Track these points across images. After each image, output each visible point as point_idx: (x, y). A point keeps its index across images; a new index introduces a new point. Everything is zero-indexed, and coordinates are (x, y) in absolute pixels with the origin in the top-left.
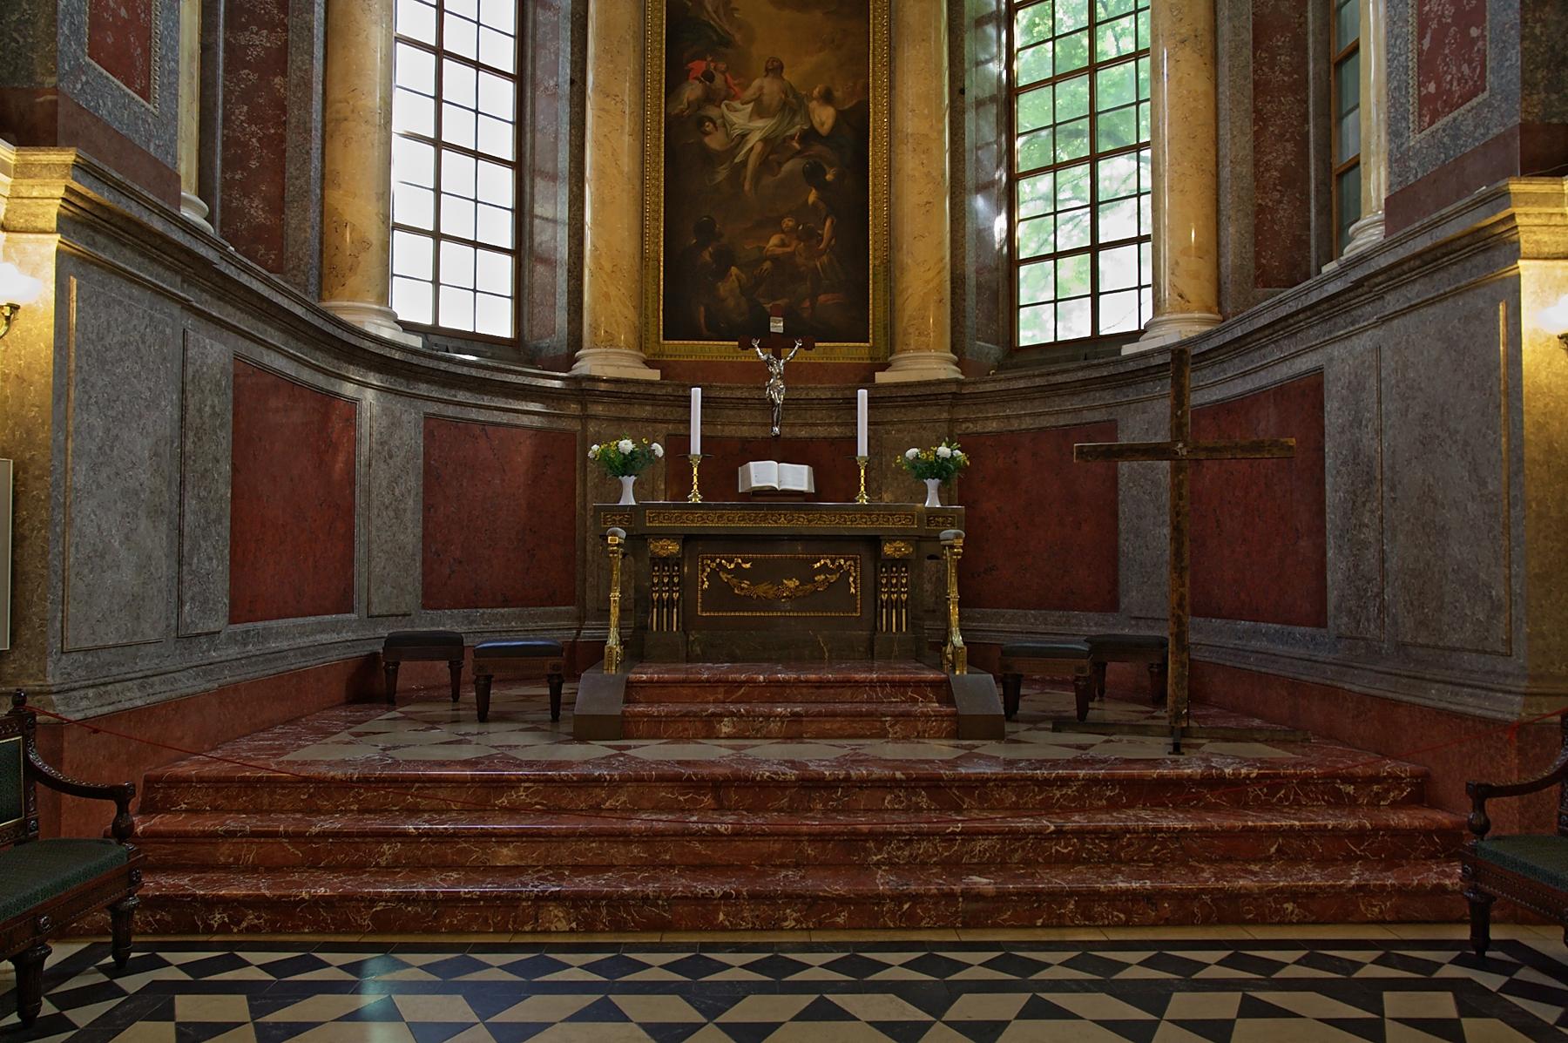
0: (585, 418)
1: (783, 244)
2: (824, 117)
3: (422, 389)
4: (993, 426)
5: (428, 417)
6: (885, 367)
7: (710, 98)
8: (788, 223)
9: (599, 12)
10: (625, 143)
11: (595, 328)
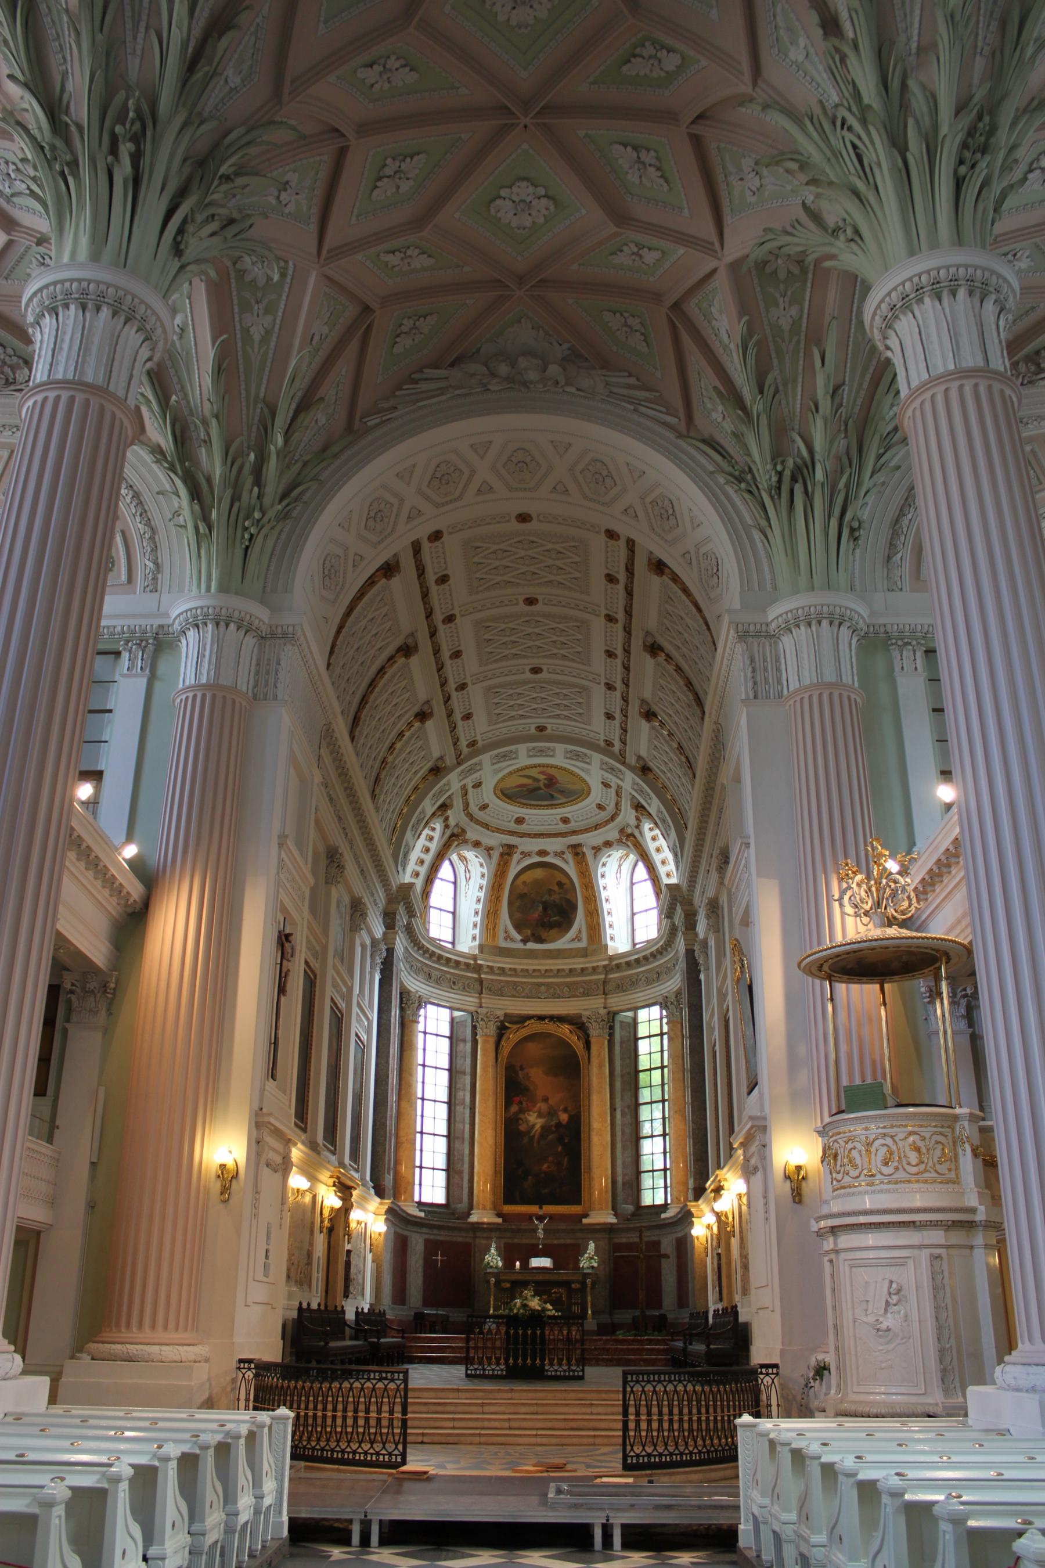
0: (475, 1237)
1: (548, 1167)
2: (564, 1117)
3: (424, 1230)
4: (624, 1240)
6: (586, 1216)
7: (521, 1111)
8: (550, 1159)
10: (490, 1133)
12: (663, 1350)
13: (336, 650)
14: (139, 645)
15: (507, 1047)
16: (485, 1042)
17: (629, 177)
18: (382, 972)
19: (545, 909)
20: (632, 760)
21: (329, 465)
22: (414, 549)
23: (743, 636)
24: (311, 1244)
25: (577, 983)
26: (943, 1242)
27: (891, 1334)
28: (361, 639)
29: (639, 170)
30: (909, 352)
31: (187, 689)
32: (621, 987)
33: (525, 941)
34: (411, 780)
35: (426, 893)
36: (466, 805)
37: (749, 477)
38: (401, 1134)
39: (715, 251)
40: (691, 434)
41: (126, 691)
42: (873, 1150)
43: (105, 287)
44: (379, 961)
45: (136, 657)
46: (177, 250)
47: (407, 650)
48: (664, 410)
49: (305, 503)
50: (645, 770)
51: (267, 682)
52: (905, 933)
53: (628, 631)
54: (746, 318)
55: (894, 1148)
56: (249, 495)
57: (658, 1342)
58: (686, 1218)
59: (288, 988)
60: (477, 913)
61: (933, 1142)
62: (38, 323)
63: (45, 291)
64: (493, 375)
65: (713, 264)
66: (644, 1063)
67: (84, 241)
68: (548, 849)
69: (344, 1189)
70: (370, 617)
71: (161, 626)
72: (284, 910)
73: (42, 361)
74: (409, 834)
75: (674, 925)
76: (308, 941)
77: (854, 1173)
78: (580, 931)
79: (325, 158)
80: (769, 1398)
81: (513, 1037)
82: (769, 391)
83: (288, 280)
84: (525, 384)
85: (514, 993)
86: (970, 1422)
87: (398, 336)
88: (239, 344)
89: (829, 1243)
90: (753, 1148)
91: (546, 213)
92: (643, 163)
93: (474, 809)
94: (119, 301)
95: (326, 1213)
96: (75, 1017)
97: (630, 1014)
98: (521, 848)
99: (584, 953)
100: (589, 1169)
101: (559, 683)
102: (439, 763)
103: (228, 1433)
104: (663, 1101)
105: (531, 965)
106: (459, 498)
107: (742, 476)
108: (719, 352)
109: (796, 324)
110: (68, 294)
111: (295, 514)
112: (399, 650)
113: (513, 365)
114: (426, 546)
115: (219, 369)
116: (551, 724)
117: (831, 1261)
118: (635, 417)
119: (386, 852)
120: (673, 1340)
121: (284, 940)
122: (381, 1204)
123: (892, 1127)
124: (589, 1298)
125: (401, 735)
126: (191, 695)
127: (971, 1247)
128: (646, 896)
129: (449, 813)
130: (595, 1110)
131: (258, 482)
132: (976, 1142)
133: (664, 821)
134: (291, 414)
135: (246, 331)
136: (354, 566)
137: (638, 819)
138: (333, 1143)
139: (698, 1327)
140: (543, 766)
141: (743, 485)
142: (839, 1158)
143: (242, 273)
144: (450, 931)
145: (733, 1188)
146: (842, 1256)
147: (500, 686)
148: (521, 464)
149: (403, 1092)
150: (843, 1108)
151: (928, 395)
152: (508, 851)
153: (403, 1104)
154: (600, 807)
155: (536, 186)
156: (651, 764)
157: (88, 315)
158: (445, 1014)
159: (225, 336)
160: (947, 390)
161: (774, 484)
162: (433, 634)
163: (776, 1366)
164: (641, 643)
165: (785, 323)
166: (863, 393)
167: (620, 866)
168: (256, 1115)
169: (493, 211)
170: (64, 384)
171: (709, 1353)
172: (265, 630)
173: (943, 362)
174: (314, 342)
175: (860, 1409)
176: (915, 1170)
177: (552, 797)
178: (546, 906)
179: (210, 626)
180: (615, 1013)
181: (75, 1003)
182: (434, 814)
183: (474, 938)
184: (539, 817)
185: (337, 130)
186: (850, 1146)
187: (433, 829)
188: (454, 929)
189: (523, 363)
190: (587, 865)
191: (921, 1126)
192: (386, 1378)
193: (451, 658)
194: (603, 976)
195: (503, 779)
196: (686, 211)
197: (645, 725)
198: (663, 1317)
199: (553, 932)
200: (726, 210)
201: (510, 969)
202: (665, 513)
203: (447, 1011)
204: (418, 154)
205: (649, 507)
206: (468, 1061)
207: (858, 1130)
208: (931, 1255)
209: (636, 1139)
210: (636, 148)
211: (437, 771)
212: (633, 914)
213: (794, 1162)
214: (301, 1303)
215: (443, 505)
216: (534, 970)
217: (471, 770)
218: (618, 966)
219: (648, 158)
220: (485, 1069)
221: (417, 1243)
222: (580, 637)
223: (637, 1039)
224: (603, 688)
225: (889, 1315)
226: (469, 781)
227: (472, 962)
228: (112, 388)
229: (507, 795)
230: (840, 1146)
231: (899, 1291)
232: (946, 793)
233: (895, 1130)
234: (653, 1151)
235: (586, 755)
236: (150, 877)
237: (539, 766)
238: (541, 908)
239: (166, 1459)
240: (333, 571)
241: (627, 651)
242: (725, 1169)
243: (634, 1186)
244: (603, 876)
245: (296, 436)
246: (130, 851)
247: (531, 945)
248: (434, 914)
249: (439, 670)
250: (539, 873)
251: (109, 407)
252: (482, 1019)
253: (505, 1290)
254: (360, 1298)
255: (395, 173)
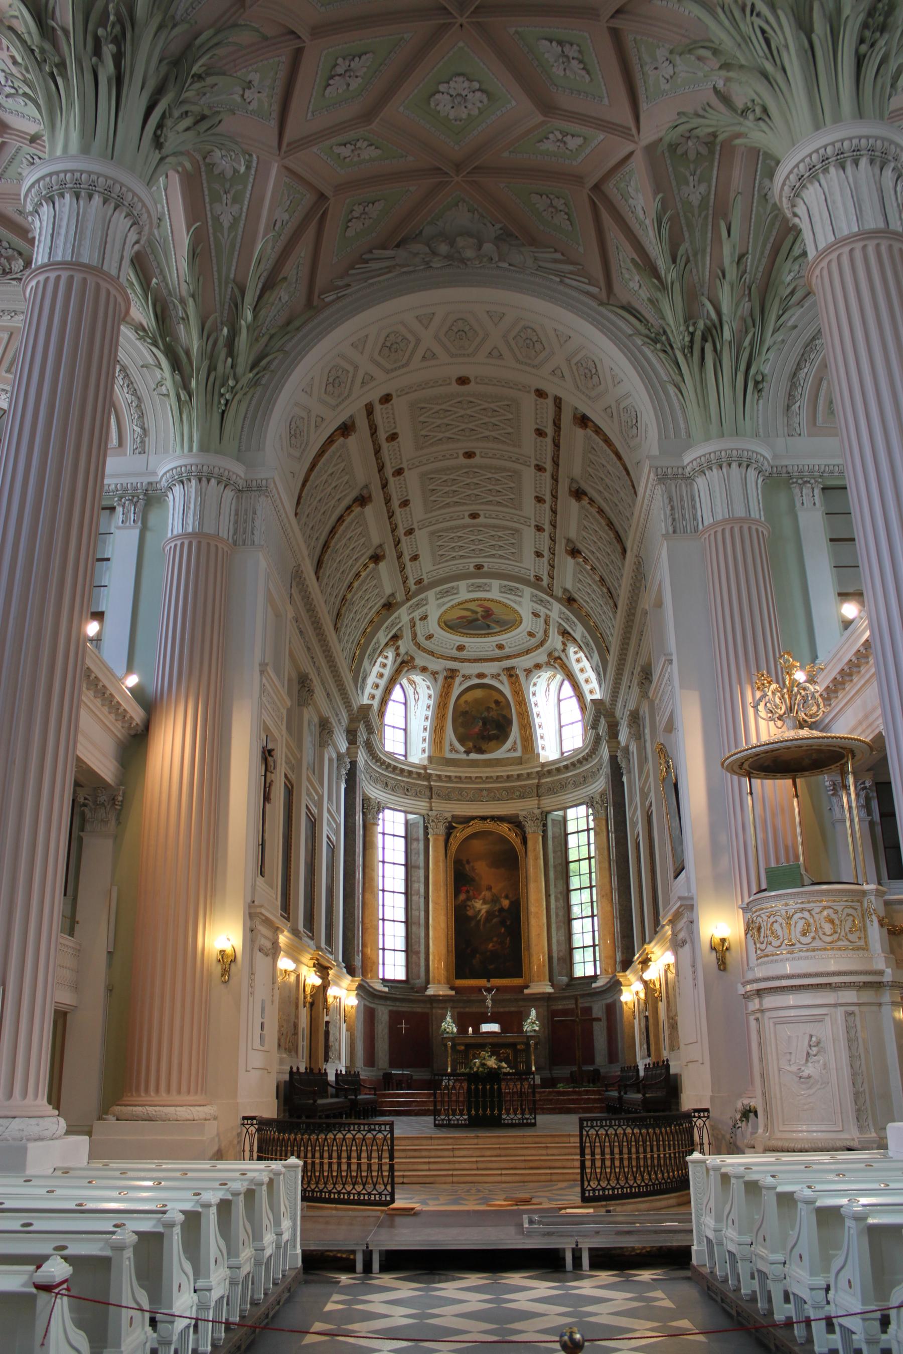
0: (432, 1008)
1: (493, 946)
2: (506, 903)
3: (389, 1003)
4: (560, 1007)
5: (391, 1012)
6: (527, 987)
7: (468, 899)
8: (495, 939)
9: (433, 877)
10: (442, 918)
11: (434, 978)
12: (599, 1099)
13: (302, 501)
14: (132, 500)
15: (454, 844)
16: (435, 840)
17: (554, 69)
18: (347, 782)
19: (484, 724)
20: (559, 593)
21: (292, 338)
22: (367, 410)
23: (663, 478)
24: (297, 1017)
25: (514, 787)
26: (855, 1000)
27: (812, 1081)
28: (322, 491)
29: (563, 63)
30: (816, 218)
31: (175, 538)
32: (552, 790)
33: (467, 752)
34: (367, 614)
35: (382, 713)
36: (415, 636)
37: (664, 338)
38: (367, 921)
39: (633, 136)
40: (611, 302)
41: (121, 541)
42: (793, 922)
43: (96, 177)
44: (344, 772)
45: (129, 511)
46: (158, 143)
47: (362, 500)
48: (586, 281)
49: (272, 371)
50: (570, 601)
51: (245, 529)
52: (816, 733)
53: (555, 479)
54: (660, 195)
55: (811, 920)
56: (223, 365)
57: (594, 1093)
58: (615, 986)
59: (272, 796)
60: (425, 729)
61: (845, 915)
62: (37, 212)
63: (42, 183)
64: (434, 253)
65: (629, 147)
66: (573, 855)
67: (75, 135)
68: (486, 672)
69: (322, 969)
70: (330, 472)
71: (150, 484)
72: (266, 729)
73: (42, 245)
74: (366, 662)
75: (598, 734)
76: (286, 756)
77: (776, 943)
78: (515, 743)
79: (283, 59)
80: (701, 1138)
81: (460, 835)
82: (681, 262)
83: (253, 171)
84: (463, 261)
85: (460, 797)
86: (890, 1153)
87: (350, 221)
88: (211, 231)
89: (754, 1004)
90: (681, 924)
91: (480, 105)
92: (567, 57)
93: (421, 639)
94: (109, 189)
95: (308, 990)
96: (88, 827)
97: (560, 813)
98: (462, 672)
99: (519, 761)
100: (528, 948)
101: (494, 526)
102: (391, 599)
103: (252, 1181)
104: (591, 887)
105: (473, 772)
106: (406, 365)
107: (658, 338)
108: (635, 227)
109: (704, 199)
110: (63, 184)
111: (264, 381)
112: (356, 500)
113: (452, 244)
114: (378, 408)
115: (193, 254)
116: (489, 564)
117: (757, 1019)
118: (561, 288)
119: (347, 677)
120: (607, 1091)
121: (267, 755)
122: (352, 981)
123: (809, 902)
124: (533, 1057)
125: (358, 575)
126: (179, 543)
127: (880, 1004)
128: (572, 710)
129: (400, 642)
130: (532, 897)
131: (231, 353)
132: (882, 913)
133: (587, 645)
134: (258, 293)
135: (216, 219)
136: (316, 426)
137: (564, 644)
138: (311, 930)
139: (629, 1079)
140: (481, 599)
141: (659, 346)
142: (762, 930)
143: (211, 166)
144: (403, 746)
145: (660, 960)
146: (767, 1014)
147: (442, 530)
148: (461, 333)
149: (367, 885)
150: (764, 886)
151: (834, 256)
152: (451, 674)
153: (367, 895)
154: (531, 634)
155: (471, 81)
156: (576, 596)
157: (81, 202)
158: (400, 817)
159: (198, 224)
160: (851, 250)
161: (687, 344)
162: (385, 486)
163: (707, 1110)
164: (567, 489)
165: (695, 199)
166: (764, 261)
167: (548, 685)
168: (250, 907)
169: (432, 105)
170: (64, 265)
171: (645, 1101)
172: (241, 483)
173: (848, 226)
174: (277, 228)
175: (786, 1145)
176: (829, 939)
177: (489, 627)
178: (485, 722)
179: (193, 482)
180: (548, 813)
181: (88, 814)
182: (387, 644)
183: (424, 751)
184: (477, 645)
185: (293, 33)
186: (772, 919)
187: (386, 657)
188: (406, 743)
189: (461, 242)
190: (520, 685)
191: (834, 901)
192: (374, 1130)
193: (400, 506)
194: (536, 781)
195: (445, 612)
196: (606, 101)
197: (570, 561)
198: (597, 1072)
199: (492, 744)
200: (642, 97)
201: (456, 777)
202: (589, 373)
203: (402, 815)
204: (366, 54)
205: (574, 368)
206: (422, 857)
207: (779, 905)
208: (846, 1012)
209: (568, 920)
210: (560, 43)
211: (389, 606)
212: (561, 727)
213: (718, 936)
214: (291, 1068)
215: (392, 370)
216: (476, 778)
217: (418, 605)
218: (549, 772)
219: (572, 52)
220: (436, 862)
221: (383, 1014)
222: (512, 485)
223: (566, 835)
224: (533, 529)
225: (809, 1064)
226: (417, 615)
227: (423, 772)
228: (105, 268)
229: (450, 626)
230: (763, 919)
231: (818, 1043)
232: (850, 610)
233: (812, 905)
234: (583, 932)
235: (518, 589)
236: (150, 704)
237: (478, 600)
238: (481, 724)
239: (207, 1206)
240: (298, 432)
241: (554, 496)
242: (652, 944)
243: (568, 961)
244: (534, 694)
245: (263, 313)
246: (132, 680)
247: (473, 756)
248: (388, 732)
249: (390, 518)
250: (478, 693)
251: (104, 285)
252: (433, 821)
253: (460, 1051)
254: (337, 1062)
255: (345, 72)
